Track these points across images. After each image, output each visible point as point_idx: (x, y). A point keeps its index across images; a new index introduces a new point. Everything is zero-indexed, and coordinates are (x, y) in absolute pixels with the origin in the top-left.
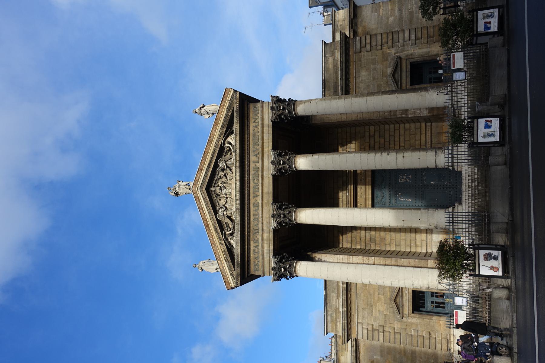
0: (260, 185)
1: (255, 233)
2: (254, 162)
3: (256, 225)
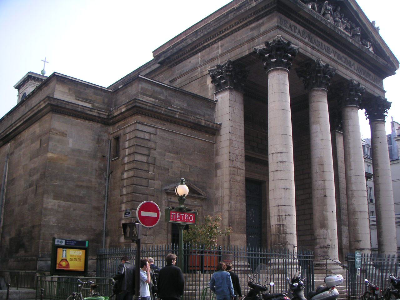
2: (354, 64)
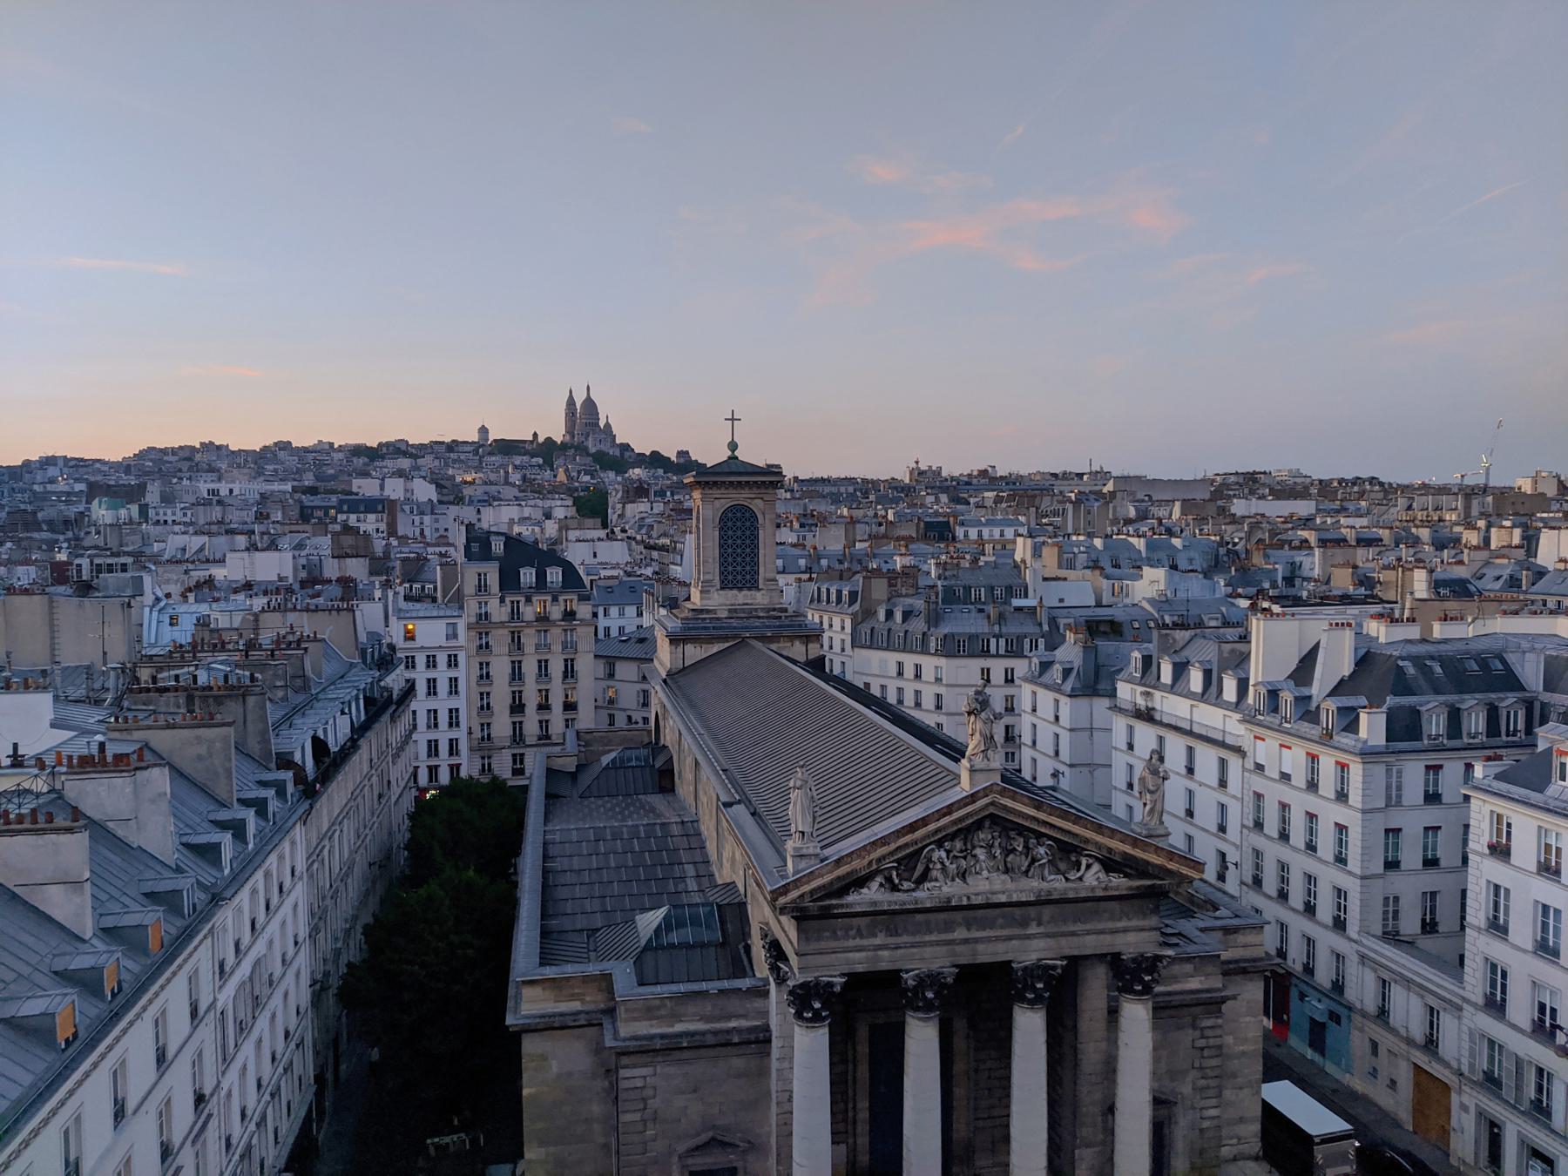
0: (991, 933)
1: (888, 929)
3: (907, 932)
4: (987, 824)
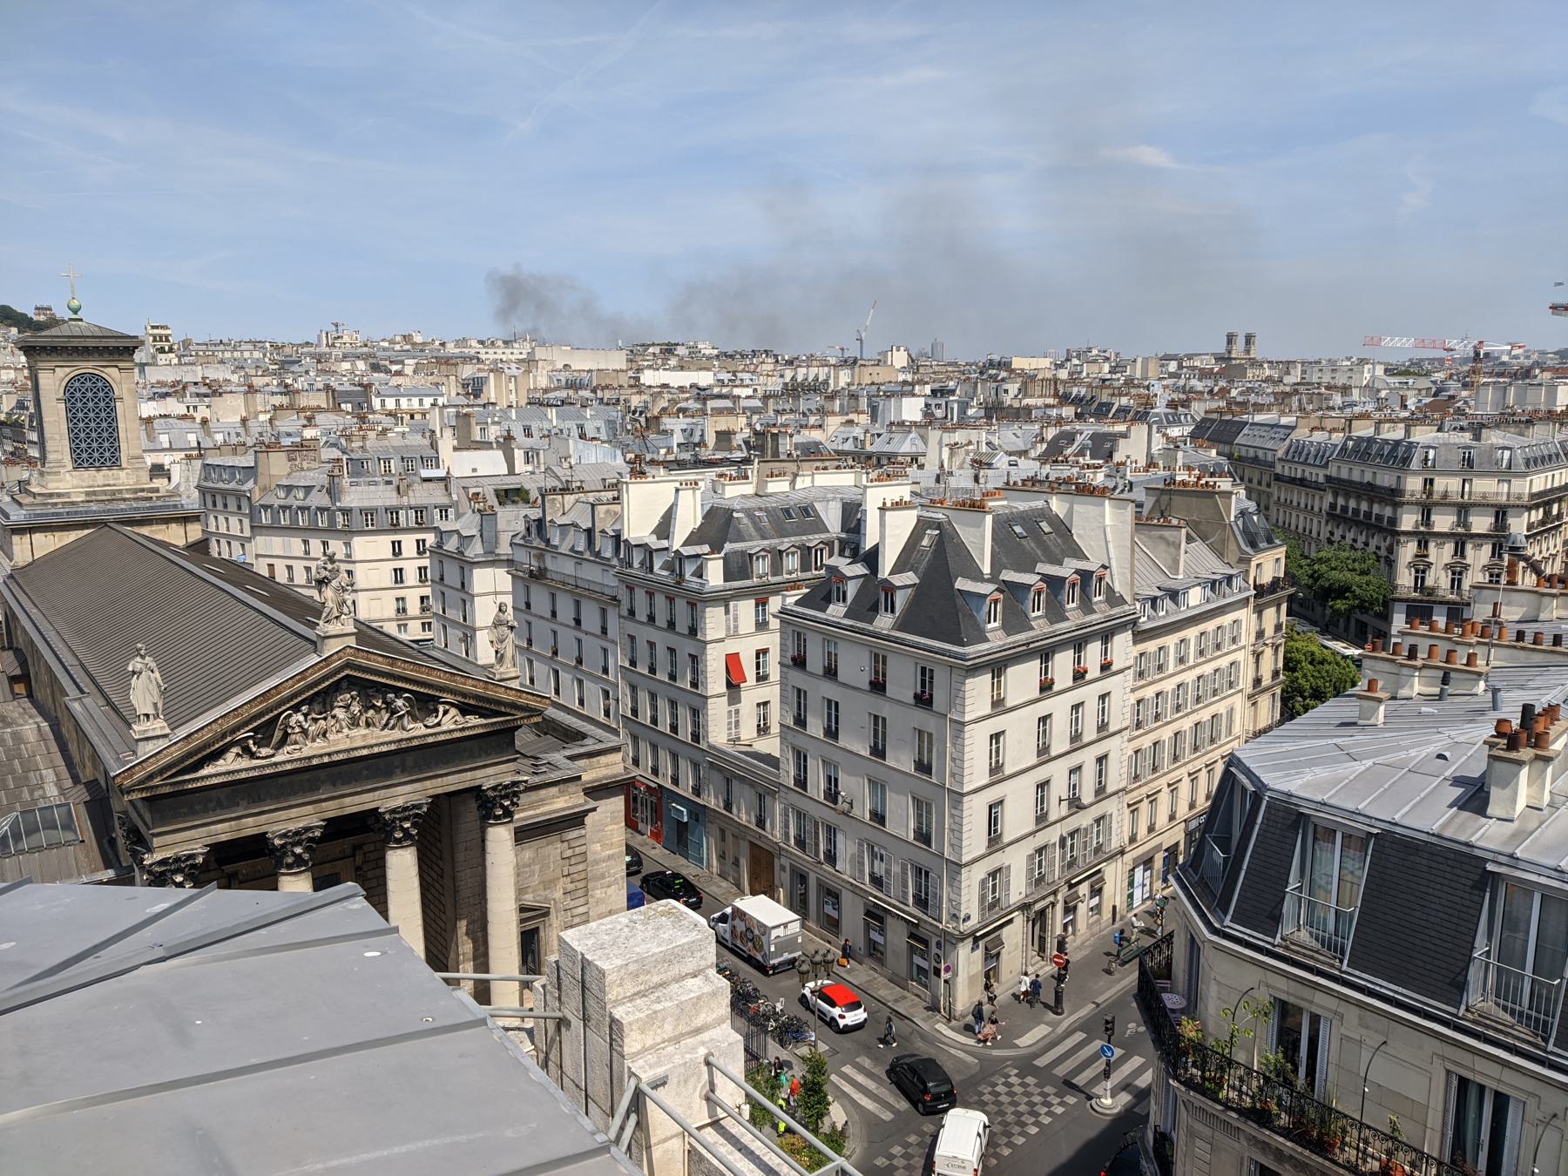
4: (344, 685)
